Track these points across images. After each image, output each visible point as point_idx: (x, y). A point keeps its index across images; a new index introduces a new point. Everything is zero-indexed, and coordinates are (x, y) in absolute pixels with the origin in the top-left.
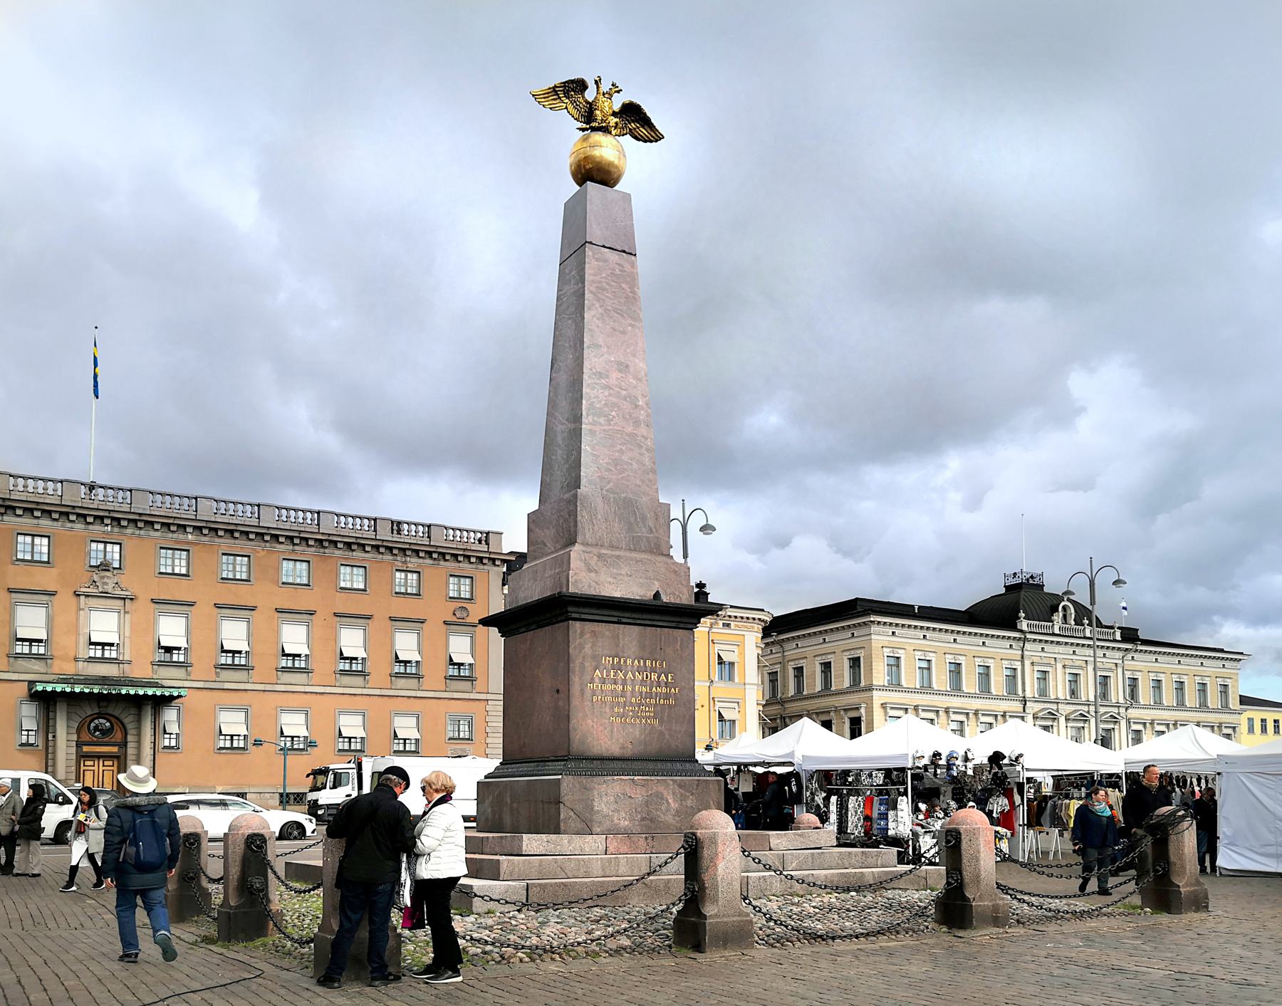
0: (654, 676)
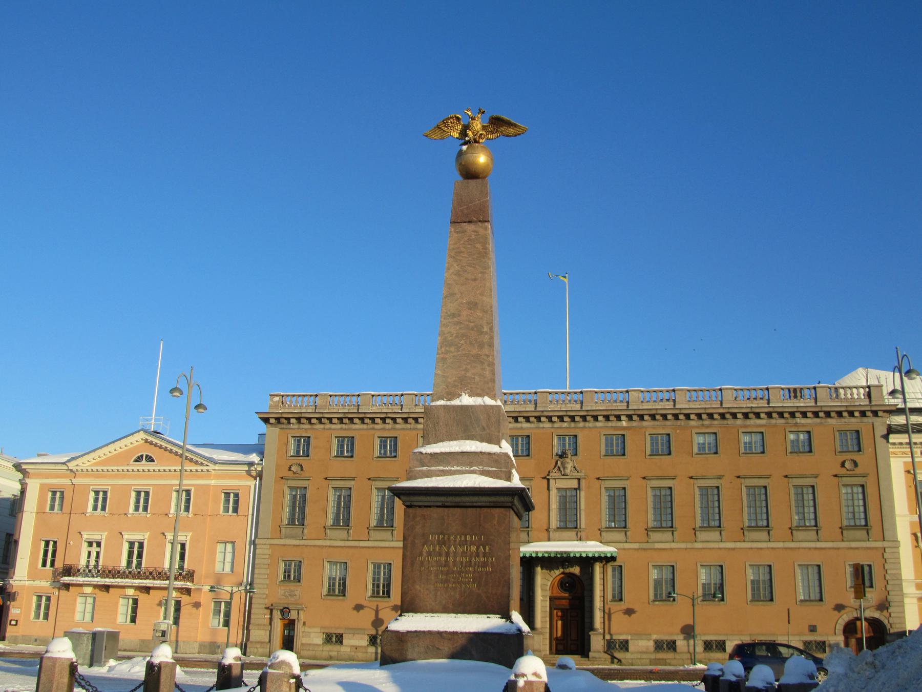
0: (473, 548)
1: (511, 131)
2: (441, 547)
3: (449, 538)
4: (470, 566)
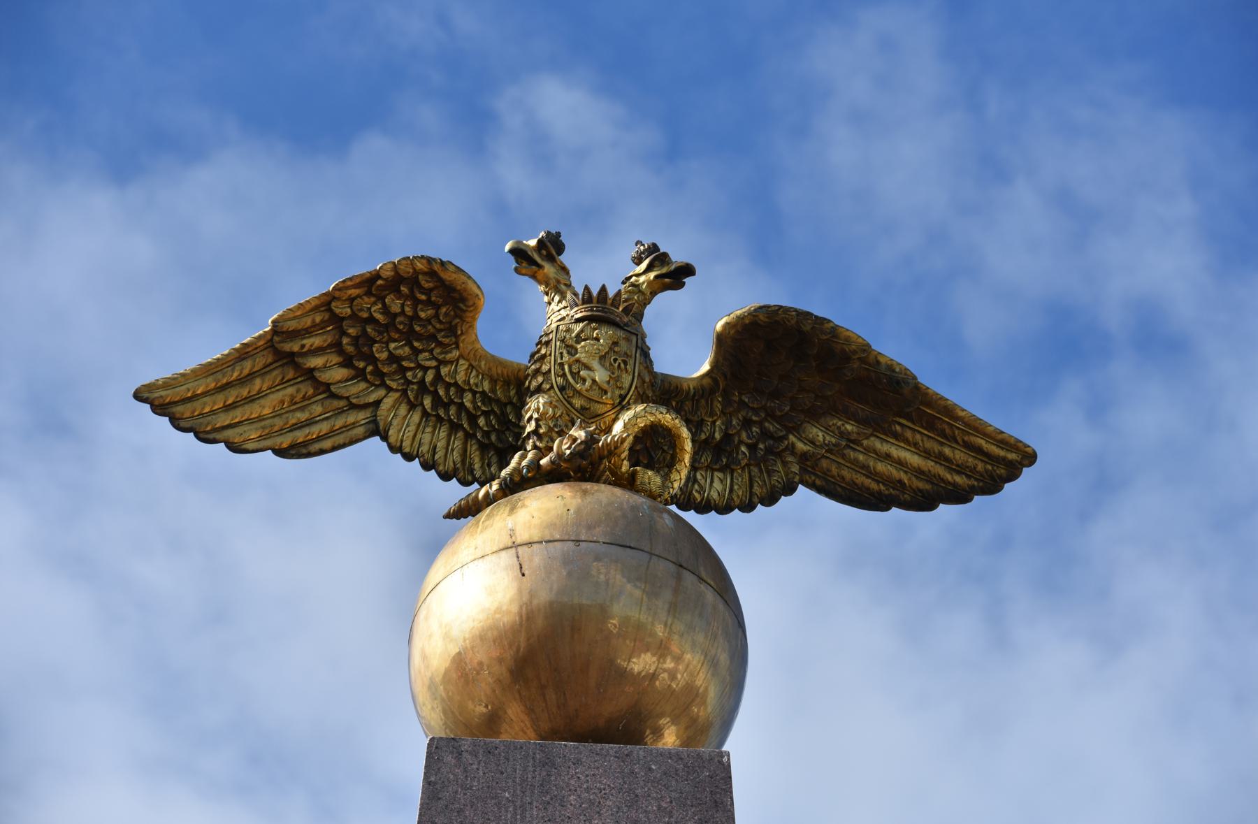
1: (902, 455)
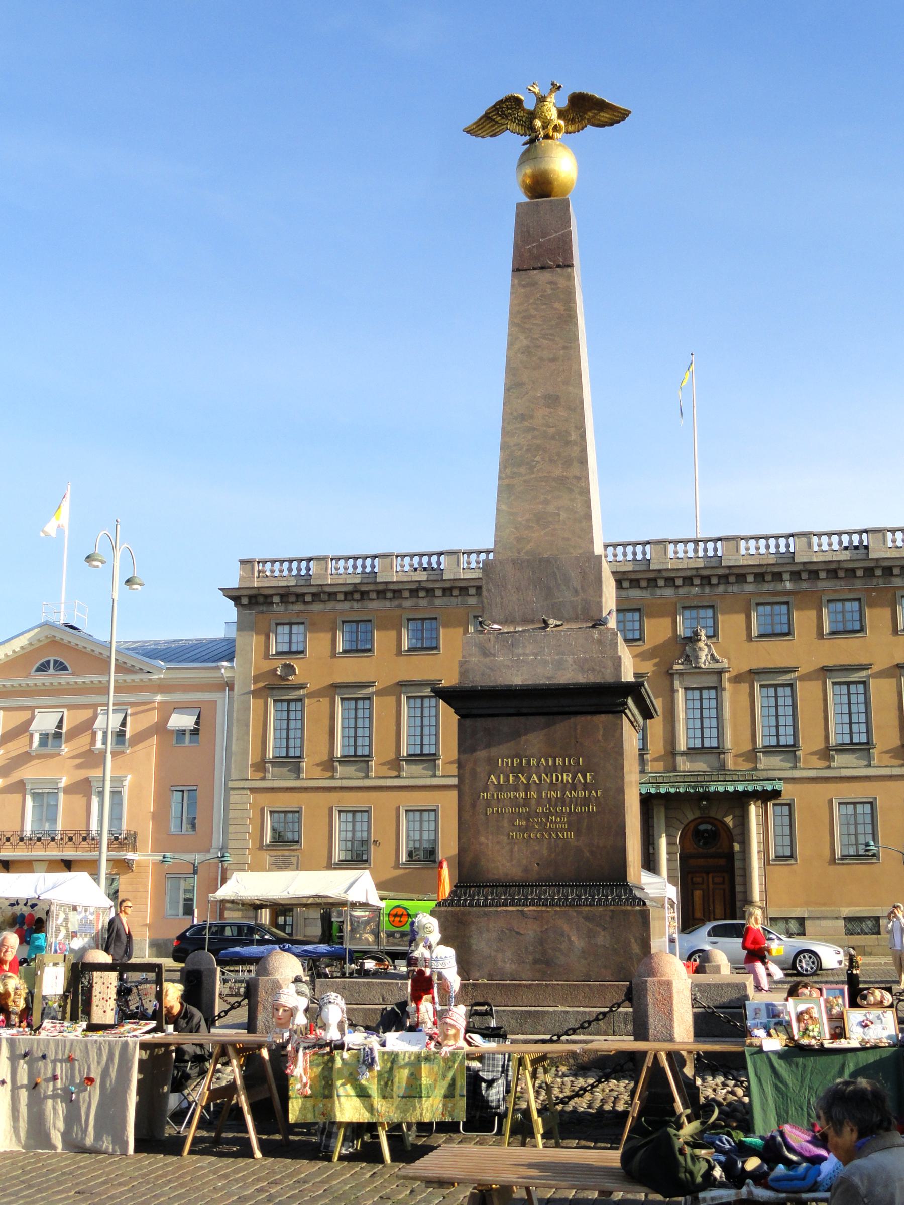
0: (567, 778)
2: (517, 778)
3: (529, 762)
4: (563, 805)
